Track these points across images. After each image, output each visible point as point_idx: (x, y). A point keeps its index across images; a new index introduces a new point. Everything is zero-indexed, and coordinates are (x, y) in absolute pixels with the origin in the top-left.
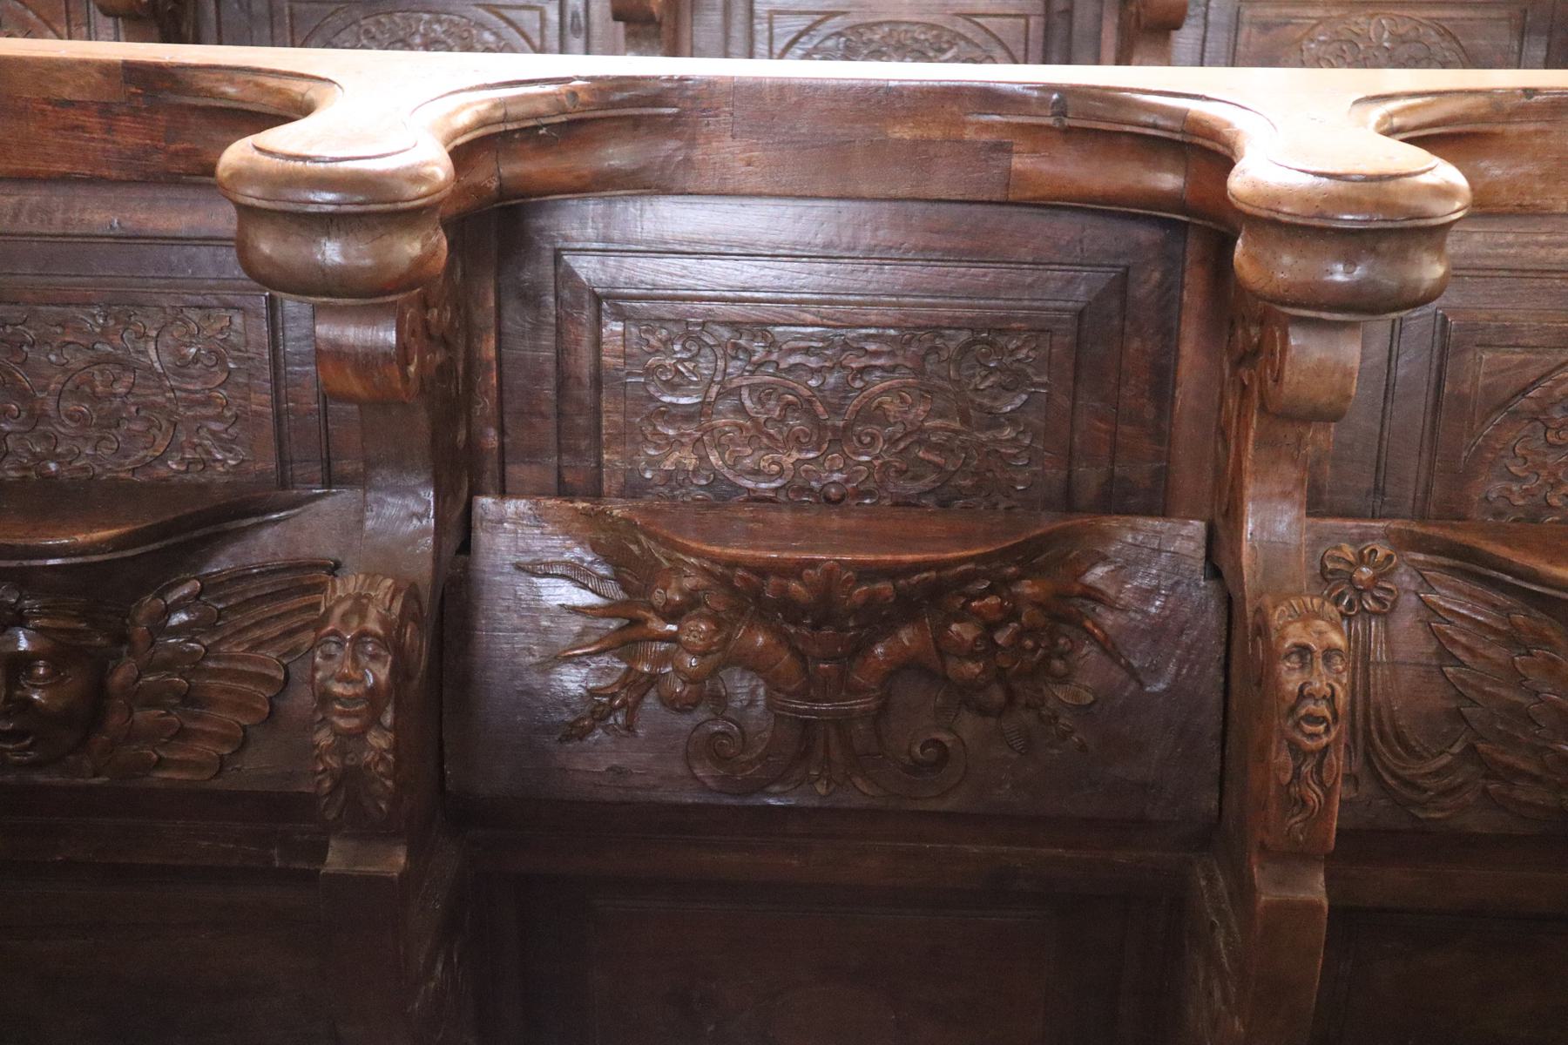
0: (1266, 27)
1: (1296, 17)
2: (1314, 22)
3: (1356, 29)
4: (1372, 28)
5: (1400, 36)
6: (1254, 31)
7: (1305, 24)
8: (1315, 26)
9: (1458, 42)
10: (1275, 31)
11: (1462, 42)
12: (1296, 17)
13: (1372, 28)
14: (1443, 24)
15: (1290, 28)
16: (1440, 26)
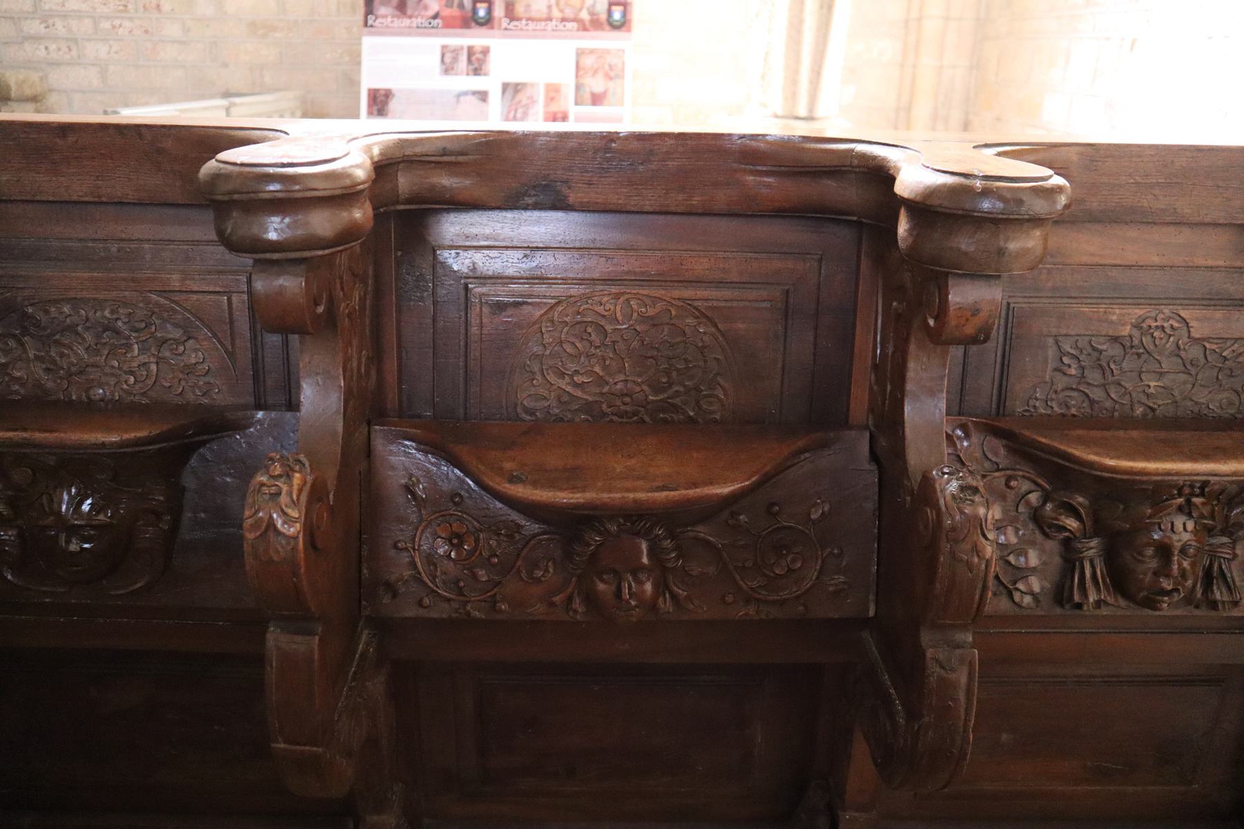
0: (500, 307)
1: (530, 296)
2: (553, 301)
3: (600, 309)
4: (618, 308)
5: (652, 318)
6: (486, 310)
7: (545, 303)
8: (552, 307)
9: (716, 326)
10: (510, 311)
11: (719, 325)
12: (530, 296)
13: (618, 308)
14: (696, 304)
15: (525, 307)
16: (696, 308)
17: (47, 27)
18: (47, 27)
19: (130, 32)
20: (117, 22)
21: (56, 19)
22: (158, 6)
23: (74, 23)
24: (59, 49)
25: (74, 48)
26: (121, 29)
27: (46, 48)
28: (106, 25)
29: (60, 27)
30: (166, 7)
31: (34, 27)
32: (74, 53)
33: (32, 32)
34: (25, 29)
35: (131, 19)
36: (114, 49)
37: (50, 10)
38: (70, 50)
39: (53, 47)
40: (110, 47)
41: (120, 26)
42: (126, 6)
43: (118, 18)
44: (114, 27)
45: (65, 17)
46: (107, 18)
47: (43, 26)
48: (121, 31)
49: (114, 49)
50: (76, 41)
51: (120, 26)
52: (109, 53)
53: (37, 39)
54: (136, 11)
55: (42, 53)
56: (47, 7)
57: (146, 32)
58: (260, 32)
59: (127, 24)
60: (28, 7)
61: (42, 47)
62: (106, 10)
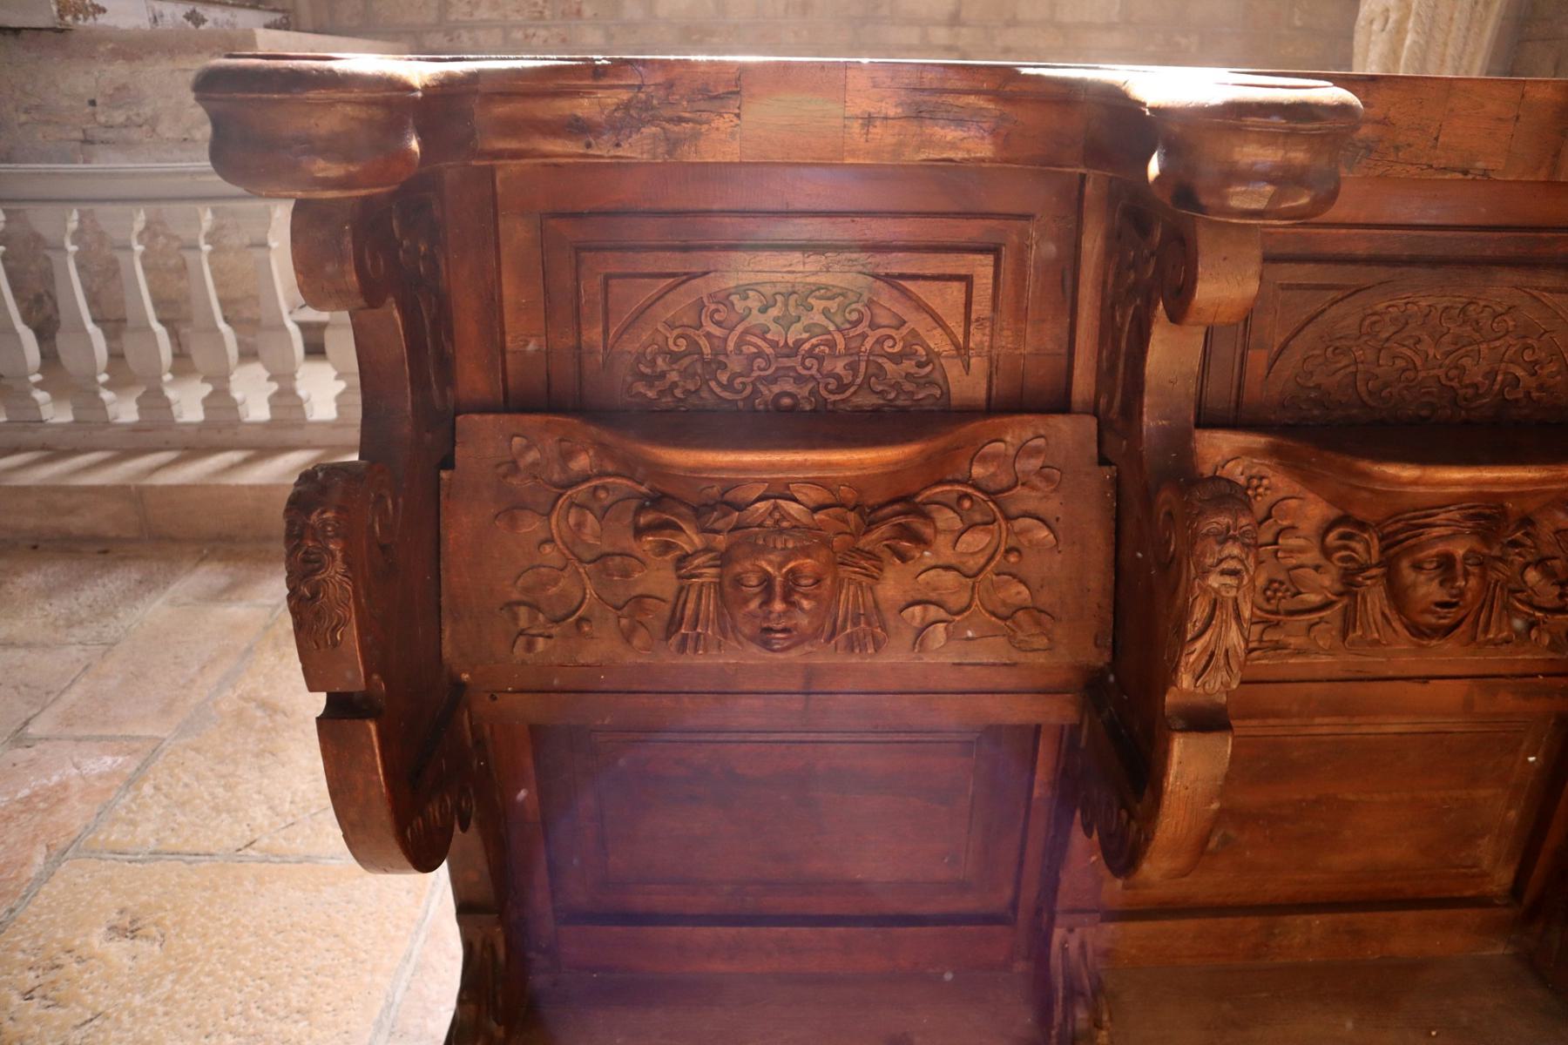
17: (451, 40)
18: (451, 40)
19: (545, 41)
20: (531, 31)
21: (462, 31)
26: (535, 39)
28: (518, 35)
35: (546, 27)
37: (457, 21)
41: (534, 35)
42: (541, 12)
43: (531, 26)
44: (526, 37)
45: (471, 28)
46: (519, 27)
47: (448, 38)
51: (534, 35)
56: (453, 18)
57: (564, 40)
59: (543, 33)
60: (431, 17)
62: (520, 18)
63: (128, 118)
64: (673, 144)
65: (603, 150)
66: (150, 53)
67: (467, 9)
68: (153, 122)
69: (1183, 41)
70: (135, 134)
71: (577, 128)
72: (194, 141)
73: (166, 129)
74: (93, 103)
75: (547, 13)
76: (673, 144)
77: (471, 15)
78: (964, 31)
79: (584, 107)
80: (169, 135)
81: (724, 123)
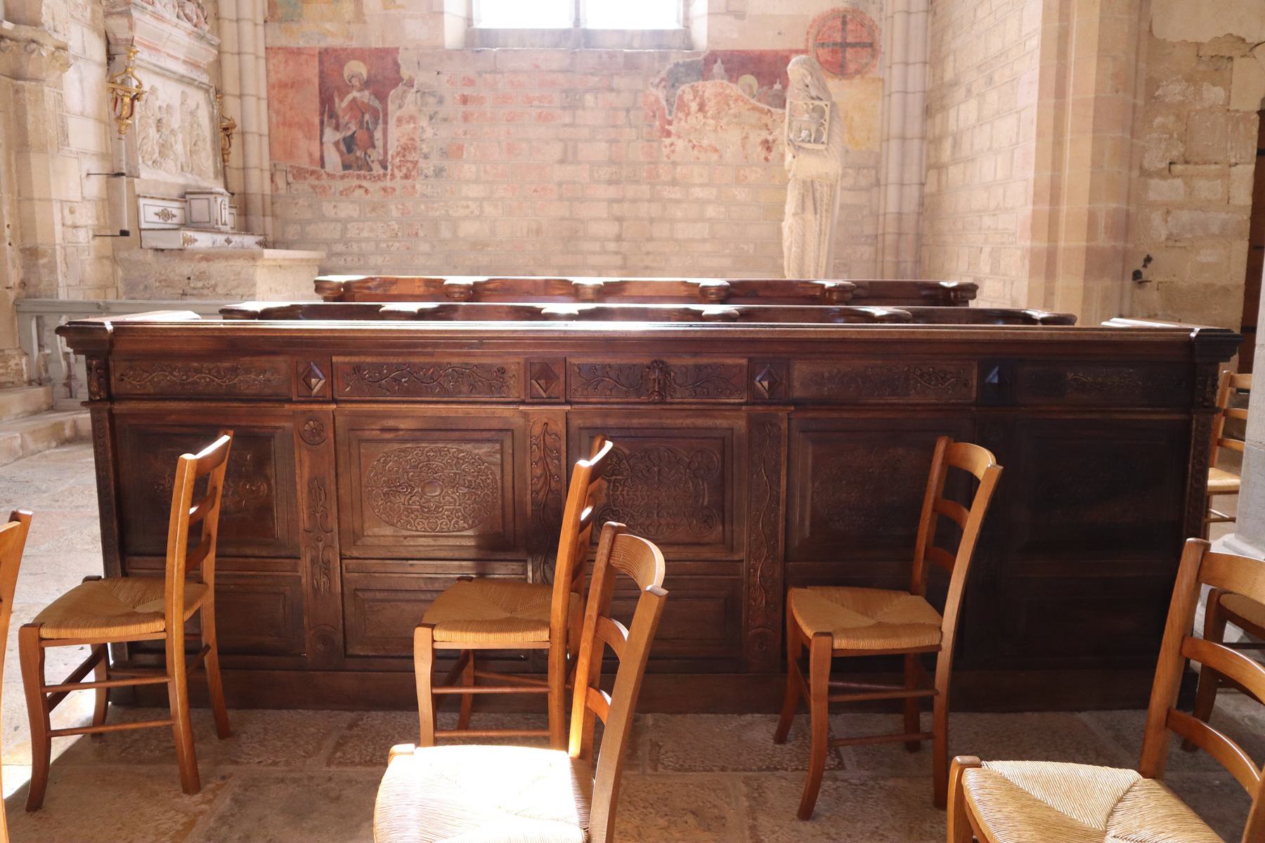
19: (398, 249)
20: (390, 244)
21: (353, 243)
22: (417, 233)
23: (363, 245)
24: (353, 260)
25: (362, 259)
27: (345, 260)
28: (384, 245)
29: (355, 248)
30: (421, 233)
31: (340, 248)
32: (362, 262)
33: (338, 250)
34: (334, 249)
35: (399, 241)
36: (387, 259)
37: (351, 237)
38: (359, 260)
39: (349, 259)
40: (385, 258)
44: (388, 246)
45: (359, 241)
46: (384, 241)
48: (392, 249)
49: (387, 259)
50: (363, 255)
52: (384, 261)
53: (339, 254)
54: (403, 236)
55: (342, 262)
56: (349, 236)
57: (408, 249)
58: (479, 247)
59: (397, 244)
61: (343, 259)
62: (385, 237)
63: (204, 285)
64: (386, 291)
65: (373, 292)
66: (218, 258)
67: (357, 231)
68: (214, 287)
69: (746, 247)
70: (206, 292)
71: (369, 288)
72: (231, 295)
73: (220, 290)
74: (189, 278)
75: (399, 234)
76: (386, 291)
77: (359, 234)
78: (624, 243)
79: (370, 284)
80: (221, 292)
81: (394, 287)
